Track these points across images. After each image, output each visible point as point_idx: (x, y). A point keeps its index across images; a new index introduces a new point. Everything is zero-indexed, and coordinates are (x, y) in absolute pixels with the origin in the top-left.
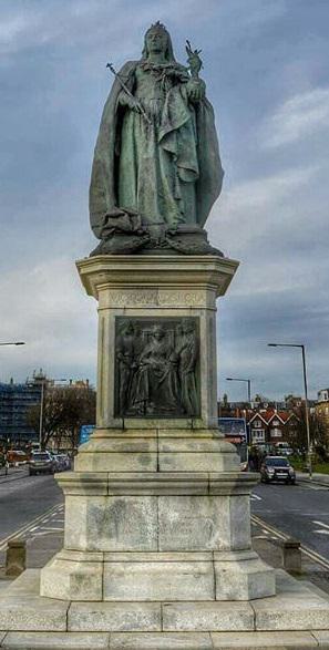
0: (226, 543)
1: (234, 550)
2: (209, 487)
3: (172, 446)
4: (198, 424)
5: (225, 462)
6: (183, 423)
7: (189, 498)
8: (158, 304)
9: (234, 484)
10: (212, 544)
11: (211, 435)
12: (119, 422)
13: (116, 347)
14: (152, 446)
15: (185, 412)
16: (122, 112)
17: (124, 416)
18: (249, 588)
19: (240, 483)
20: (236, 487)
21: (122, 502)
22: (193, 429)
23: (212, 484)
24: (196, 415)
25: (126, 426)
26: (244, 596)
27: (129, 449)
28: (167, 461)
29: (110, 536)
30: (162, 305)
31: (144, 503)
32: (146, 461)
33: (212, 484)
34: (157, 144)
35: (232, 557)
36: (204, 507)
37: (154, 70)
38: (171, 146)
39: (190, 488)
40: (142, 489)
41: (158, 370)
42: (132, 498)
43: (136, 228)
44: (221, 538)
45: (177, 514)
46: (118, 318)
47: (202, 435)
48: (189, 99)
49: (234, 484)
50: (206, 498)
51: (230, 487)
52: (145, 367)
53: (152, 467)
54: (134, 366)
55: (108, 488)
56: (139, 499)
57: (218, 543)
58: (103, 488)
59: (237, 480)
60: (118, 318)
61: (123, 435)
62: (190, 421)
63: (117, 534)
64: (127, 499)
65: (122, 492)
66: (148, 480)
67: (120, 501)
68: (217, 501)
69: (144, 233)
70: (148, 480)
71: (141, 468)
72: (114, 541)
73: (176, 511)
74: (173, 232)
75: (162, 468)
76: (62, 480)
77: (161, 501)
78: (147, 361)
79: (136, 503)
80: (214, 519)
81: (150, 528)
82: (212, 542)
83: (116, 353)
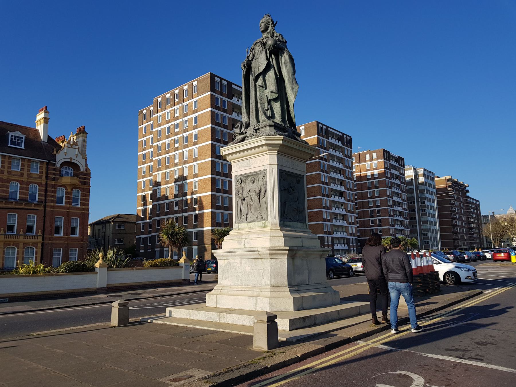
4: (267, 223)
5: (271, 241)
6: (260, 223)
21: (229, 263)
32: (240, 243)
39: (253, 255)
44: (267, 281)
45: (249, 268)
53: (242, 246)
68: (265, 260)
79: (235, 262)
81: (240, 274)
82: (263, 281)
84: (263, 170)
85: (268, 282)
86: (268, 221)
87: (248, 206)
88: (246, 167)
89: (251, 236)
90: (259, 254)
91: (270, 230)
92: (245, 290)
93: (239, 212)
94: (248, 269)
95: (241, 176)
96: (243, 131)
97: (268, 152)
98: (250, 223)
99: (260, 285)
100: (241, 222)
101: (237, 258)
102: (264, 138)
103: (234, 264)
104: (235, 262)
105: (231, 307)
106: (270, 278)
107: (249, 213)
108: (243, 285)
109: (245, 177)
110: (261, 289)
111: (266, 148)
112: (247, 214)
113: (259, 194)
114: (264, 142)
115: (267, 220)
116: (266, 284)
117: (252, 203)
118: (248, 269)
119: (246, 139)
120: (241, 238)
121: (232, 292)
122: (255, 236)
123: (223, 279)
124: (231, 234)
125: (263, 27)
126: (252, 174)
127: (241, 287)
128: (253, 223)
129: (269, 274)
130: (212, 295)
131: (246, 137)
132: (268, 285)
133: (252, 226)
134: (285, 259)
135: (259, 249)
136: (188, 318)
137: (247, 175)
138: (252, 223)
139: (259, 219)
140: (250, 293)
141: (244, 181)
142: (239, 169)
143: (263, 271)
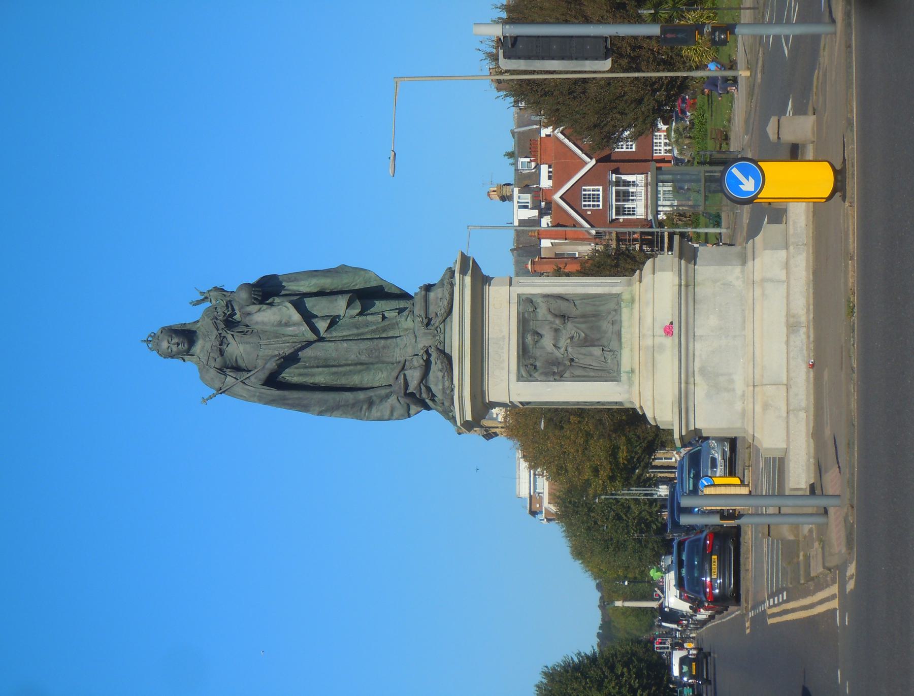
1: (744, 262)
3: (648, 321)
4: (626, 296)
6: (625, 312)
8: (504, 338)
11: (638, 283)
12: (624, 377)
13: (549, 381)
14: (649, 342)
15: (615, 310)
16: (273, 381)
17: (619, 372)
18: (776, 249)
21: (703, 370)
22: (633, 301)
23: (683, 283)
25: (628, 369)
26: (783, 253)
27: (650, 365)
29: (731, 381)
31: (701, 349)
32: (662, 348)
34: (321, 339)
35: (750, 263)
36: (701, 291)
37: (221, 345)
38: (322, 325)
41: (572, 338)
43: (421, 362)
44: (733, 273)
46: (520, 378)
47: (637, 293)
48: (260, 304)
52: (570, 350)
54: (568, 363)
59: (680, 258)
60: (520, 378)
61: (637, 371)
62: (623, 305)
65: (691, 370)
67: (699, 371)
68: (699, 278)
69: (427, 352)
74: (425, 321)
77: (698, 332)
78: (562, 350)
83: (555, 380)
84: (519, 303)
85: (738, 269)
86: (623, 294)
87: (585, 345)
94: (713, 321)
95: (521, 364)
96: (422, 358)
98: (623, 340)
100: (619, 364)
101: (691, 345)
106: (730, 267)
107: (600, 344)
109: (523, 355)
112: (603, 350)
113: (564, 317)
115: (618, 296)
116: (741, 276)
118: (713, 321)
119: (441, 348)
123: (734, 390)
126: (521, 335)
128: (622, 333)
129: (724, 268)
131: (438, 349)
132: (742, 272)
135: (677, 282)
136: (805, 415)
137: (521, 347)
138: (623, 336)
139: (616, 318)
141: (531, 360)
143: (718, 284)
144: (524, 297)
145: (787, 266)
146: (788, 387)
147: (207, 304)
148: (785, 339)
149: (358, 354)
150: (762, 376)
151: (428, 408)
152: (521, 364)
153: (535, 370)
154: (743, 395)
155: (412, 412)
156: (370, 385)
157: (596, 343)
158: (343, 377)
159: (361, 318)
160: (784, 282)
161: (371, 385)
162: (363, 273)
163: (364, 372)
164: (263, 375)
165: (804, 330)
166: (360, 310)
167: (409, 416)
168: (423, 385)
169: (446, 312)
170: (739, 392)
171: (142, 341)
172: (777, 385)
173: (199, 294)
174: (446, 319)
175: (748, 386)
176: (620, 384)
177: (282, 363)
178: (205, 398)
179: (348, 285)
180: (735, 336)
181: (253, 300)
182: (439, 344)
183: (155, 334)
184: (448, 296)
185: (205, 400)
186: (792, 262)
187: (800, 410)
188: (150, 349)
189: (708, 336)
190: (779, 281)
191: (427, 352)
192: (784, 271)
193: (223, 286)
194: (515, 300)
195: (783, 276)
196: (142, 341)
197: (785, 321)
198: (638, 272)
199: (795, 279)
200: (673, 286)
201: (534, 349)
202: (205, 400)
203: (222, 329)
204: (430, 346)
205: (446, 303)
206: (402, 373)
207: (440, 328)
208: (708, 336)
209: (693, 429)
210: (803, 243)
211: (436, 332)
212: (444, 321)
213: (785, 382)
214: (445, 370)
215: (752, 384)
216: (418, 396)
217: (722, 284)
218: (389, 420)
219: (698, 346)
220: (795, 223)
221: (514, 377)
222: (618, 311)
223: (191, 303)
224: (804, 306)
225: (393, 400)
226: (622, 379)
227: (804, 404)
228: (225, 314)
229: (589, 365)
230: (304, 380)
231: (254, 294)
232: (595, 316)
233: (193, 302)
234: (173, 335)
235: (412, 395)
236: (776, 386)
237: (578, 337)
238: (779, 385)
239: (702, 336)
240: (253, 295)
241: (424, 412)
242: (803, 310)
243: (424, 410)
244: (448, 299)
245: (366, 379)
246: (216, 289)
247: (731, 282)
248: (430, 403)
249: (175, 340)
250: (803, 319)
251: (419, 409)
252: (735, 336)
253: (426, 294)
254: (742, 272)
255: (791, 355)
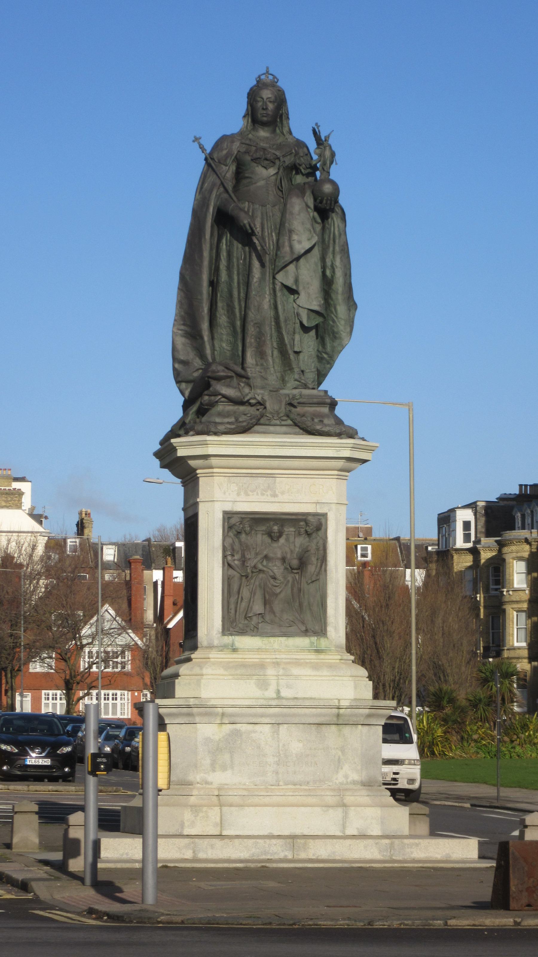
0: (355, 776)
2: (338, 715)
4: (323, 643)
5: (355, 688)
7: (314, 727)
8: (275, 495)
9: (367, 711)
10: (340, 778)
11: (339, 657)
12: (228, 640)
18: (382, 823)
19: (373, 711)
20: (369, 716)
21: (237, 734)
23: (342, 711)
24: (322, 632)
28: (288, 686)
29: (224, 768)
30: (280, 498)
32: (263, 685)
33: (342, 711)
39: (320, 715)
40: (262, 716)
42: (250, 727)
45: (301, 745)
46: (225, 513)
49: (367, 711)
50: (333, 728)
51: (362, 715)
53: (271, 693)
55: (223, 715)
56: (257, 727)
57: (346, 777)
58: (217, 714)
63: (232, 768)
64: (243, 728)
65: (238, 720)
66: (270, 707)
67: (236, 730)
68: (347, 730)
70: (270, 707)
71: (258, 693)
72: (229, 772)
73: (299, 741)
74: (295, 402)
75: (283, 694)
76: (166, 707)
77: (283, 729)
79: (255, 732)
80: (343, 750)
81: (271, 760)
86: (326, 639)
88: (263, 494)
89: (295, 671)
90: (338, 715)
91: (338, 661)
92: (297, 793)
93: (232, 606)
97: (336, 472)
99: (330, 784)
102: (351, 446)
103: (253, 735)
104: (255, 732)
105: (269, 831)
106: (359, 767)
108: (281, 783)
110: (340, 791)
111: (341, 464)
114: (347, 453)
116: (349, 780)
117: (278, 590)
119: (262, 421)
120: (261, 673)
121: (256, 800)
122: (309, 671)
123: (214, 771)
124: (194, 660)
125: (270, 113)
127: (276, 787)
130: (205, 809)
132: (354, 782)
133: (276, 646)
134: (377, 727)
135: (344, 703)
140: (311, 800)
141: (249, 529)
142: (238, 494)
143: (340, 753)
144: (323, 521)
145: (363, 836)
146: (220, 836)
147: (312, 145)
148: (276, 833)
149: (255, 322)
150: (231, 805)
151: (186, 406)
152: (243, 516)
153: (236, 533)
154: (207, 783)
155: (183, 385)
156: (216, 336)
157: (267, 606)
158: (225, 304)
159: (298, 325)
160: (343, 831)
161: (216, 337)
162: (348, 329)
163: (232, 329)
164: (231, 208)
165: (290, 857)
166: (306, 325)
167: (178, 382)
168: (220, 399)
169: (308, 427)
170: (211, 777)
171: (267, 68)
172: (221, 823)
173: (327, 134)
174: (298, 426)
175: (219, 789)
176: (220, 635)
177: (247, 231)
178: (201, 141)
179: (334, 312)
180: (277, 773)
181: (320, 198)
182: (269, 418)
183: (277, 82)
184: (326, 429)
185: (196, 139)
186: (370, 842)
187: (194, 852)
188: (259, 77)
189: (278, 741)
190: (344, 827)
191: (259, 403)
192: (356, 833)
193: (336, 164)
194: (320, 510)
195: (350, 831)
196: (267, 68)
197: (297, 834)
198: (352, 658)
199: (350, 845)
200: (339, 700)
201: (261, 532)
202: (196, 139)
203: (284, 162)
204: (265, 408)
205: (318, 427)
206: (233, 374)
207: (286, 420)
208: (278, 741)
209: (166, 723)
210: (392, 855)
211: (282, 415)
212: (296, 425)
213: (224, 833)
214: (239, 424)
215: (220, 794)
216: (206, 392)
217: (339, 757)
218: (174, 359)
219: (267, 729)
220: (417, 845)
221: (228, 507)
222: (306, 633)
223: (316, 124)
224: (319, 856)
225: (197, 363)
226: (226, 637)
227: (201, 855)
228: (300, 165)
229: (242, 598)
230: (222, 258)
231: (327, 200)
232: (301, 605)
233: (318, 127)
234: (276, 104)
235: (208, 386)
236: (219, 822)
237: (275, 584)
238: (221, 827)
239: (278, 734)
240: (325, 198)
241: (181, 400)
242: (314, 855)
243: (183, 399)
244: (323, 429)
245: (223, 332)
246: (333, 155)
247: (342, 769)
248: (194, 408)
249: (271, 106)
250: (303, 855)
251: (187, 393)
252: (277, 773)
253: (326, 404)
254: (354, 781)
255: (261, 841)
